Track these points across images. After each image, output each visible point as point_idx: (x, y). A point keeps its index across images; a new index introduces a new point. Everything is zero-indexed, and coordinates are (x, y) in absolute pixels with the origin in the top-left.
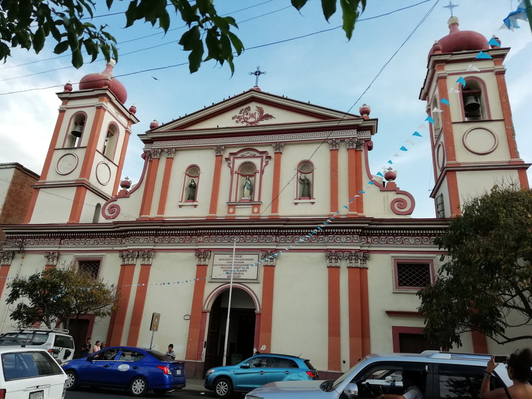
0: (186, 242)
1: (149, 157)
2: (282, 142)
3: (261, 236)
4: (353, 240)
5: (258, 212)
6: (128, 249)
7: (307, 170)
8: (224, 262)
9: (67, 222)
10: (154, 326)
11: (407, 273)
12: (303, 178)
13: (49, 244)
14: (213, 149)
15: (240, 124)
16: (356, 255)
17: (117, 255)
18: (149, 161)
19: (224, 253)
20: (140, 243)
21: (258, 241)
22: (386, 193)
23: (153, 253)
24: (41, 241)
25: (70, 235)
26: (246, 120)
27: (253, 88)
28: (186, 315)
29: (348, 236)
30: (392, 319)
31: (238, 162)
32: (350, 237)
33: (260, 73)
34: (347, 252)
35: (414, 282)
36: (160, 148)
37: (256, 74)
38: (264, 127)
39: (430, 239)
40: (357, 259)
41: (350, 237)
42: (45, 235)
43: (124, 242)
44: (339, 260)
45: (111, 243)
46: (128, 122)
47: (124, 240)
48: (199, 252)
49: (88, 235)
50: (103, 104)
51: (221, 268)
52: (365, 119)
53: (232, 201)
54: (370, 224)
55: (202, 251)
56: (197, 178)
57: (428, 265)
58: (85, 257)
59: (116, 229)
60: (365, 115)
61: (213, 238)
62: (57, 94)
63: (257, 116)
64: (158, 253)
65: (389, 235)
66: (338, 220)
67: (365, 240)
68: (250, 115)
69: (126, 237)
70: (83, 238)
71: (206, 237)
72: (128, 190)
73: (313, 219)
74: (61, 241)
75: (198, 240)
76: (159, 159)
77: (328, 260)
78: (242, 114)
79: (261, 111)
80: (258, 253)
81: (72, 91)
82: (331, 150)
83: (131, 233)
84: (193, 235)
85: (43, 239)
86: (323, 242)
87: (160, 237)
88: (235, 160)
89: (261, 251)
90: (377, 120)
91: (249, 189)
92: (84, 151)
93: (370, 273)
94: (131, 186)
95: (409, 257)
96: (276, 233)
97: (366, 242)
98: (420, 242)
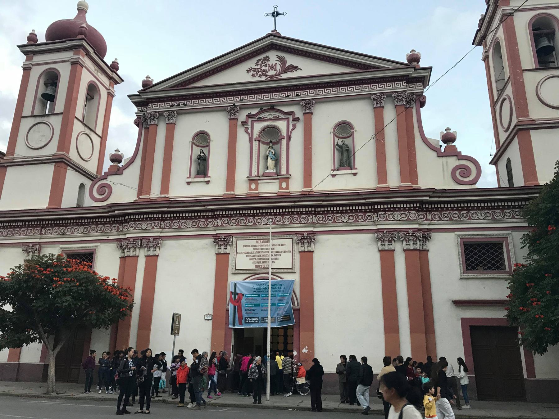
0: (200, 226)
1: (144, 123)
2: (313, 99)
3: (295, 216)
4: (410, 217)
5: (287, 187)
6: (128, 237)
7: (344, 134)
8: (250, 249)
9: (47, 207)
10: (175, 330)
11: (476, 254)
12: (340, 143)
13: (26, 235)
14: (224, 110)
15: (257, 79)
16: (414, 235)
17: (114, 245)
18: (145, 128)
19: (249, 238)
20: (143, 229)
21: (291, 223)
22: (444, 159)
23: (160, 242)
25: (53, 222)
26: (264, 73)
27: (271, 32)
28: (206, 315)
29: (403, 212)
30: (460, 309)
31: (258, 127)
32: (405, 214)
33: (278, 14)
34: (403, 232)
35: (485, 265)
36: (157, 112)
37: (273, 16)
38: (289, 81)
39: (503, 213)
40: (415, 239)
41: (405, 214)
42: (21, 224)
43: (121, 229)
44: (393, 242)
45: (106, 231)
46: (110, 82)
47: (121, 226)
48: (218, 238)
49: (76, 222)
50: (79, 58)
51: (247, 256)
52: (416, 68)
53: (253, 175)
54: (430, 197)
55: (222, 237)
56: (208, 148)
57: (502, 244)
59: (110, 213)
60: (415, 64)
61: (234, 221)
62: (19, 46)
63: (278, 67)
64: (166, 241)
65: (453, 209)
66: (388, 192)
67: (424, 216)
68: (269, 66)
70: (70, 226)
71: (225, 219)
72: (120, 165)
73: (360, 193)
74: (41, 231)
75: (216, 224)
76: (157, 125)
77: (380, 243)
78: (259, 65)
79: (283, 61)
80: (291, 237)
81: (38, 43)
82: (374, 108)
83: (129, 218)
84: (208, 217)
85: (18, 229)
86: (372, 220)
87: (167, 222)
88: (254, 124)
89: (295, 234)
90: (430, 68)
91: (273, 159)
92: (60, 118)
93: (431, 256)
94: (123, 160)
95: (478, 235)
96: (313, 212)
97: (425, 218)
98: (491, 217)
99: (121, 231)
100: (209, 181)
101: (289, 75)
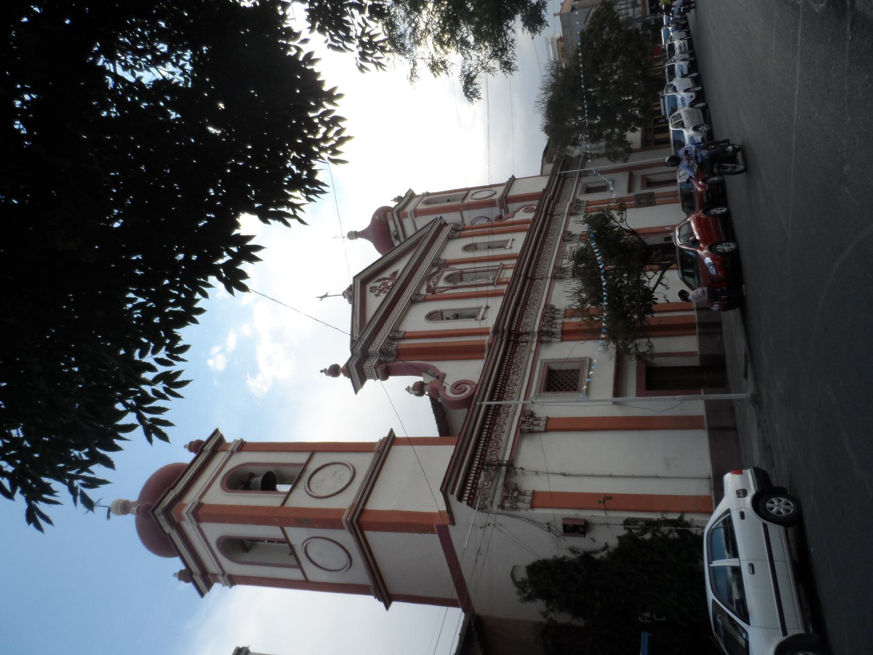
18: (395, 361)
24: (495, 444)
31: (442, 284)
33: (326, 296)
58: (540, 383)
63: (387, 281)
69: (518, 339)
70: (505, 387)
85: (492, 442)
99: (527, 344)
100: (487, 306)
101: (398, 276)
